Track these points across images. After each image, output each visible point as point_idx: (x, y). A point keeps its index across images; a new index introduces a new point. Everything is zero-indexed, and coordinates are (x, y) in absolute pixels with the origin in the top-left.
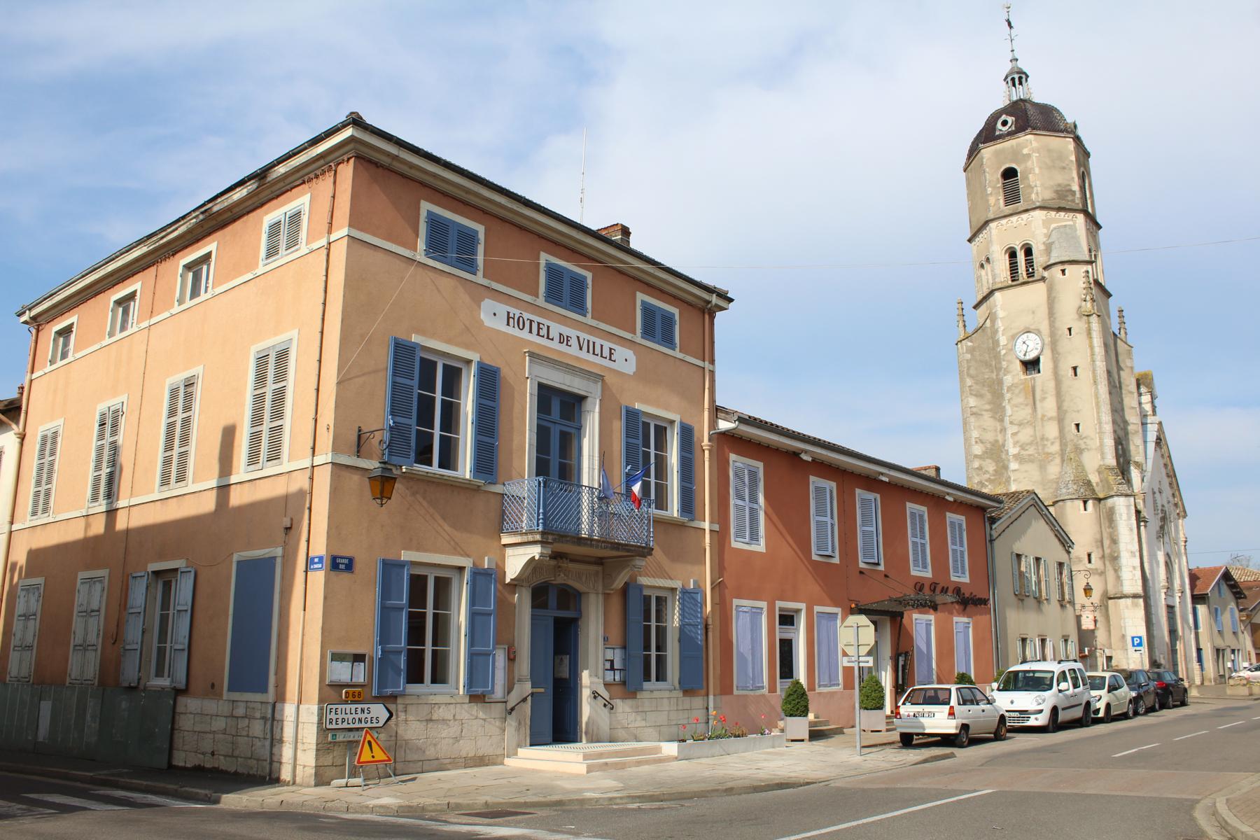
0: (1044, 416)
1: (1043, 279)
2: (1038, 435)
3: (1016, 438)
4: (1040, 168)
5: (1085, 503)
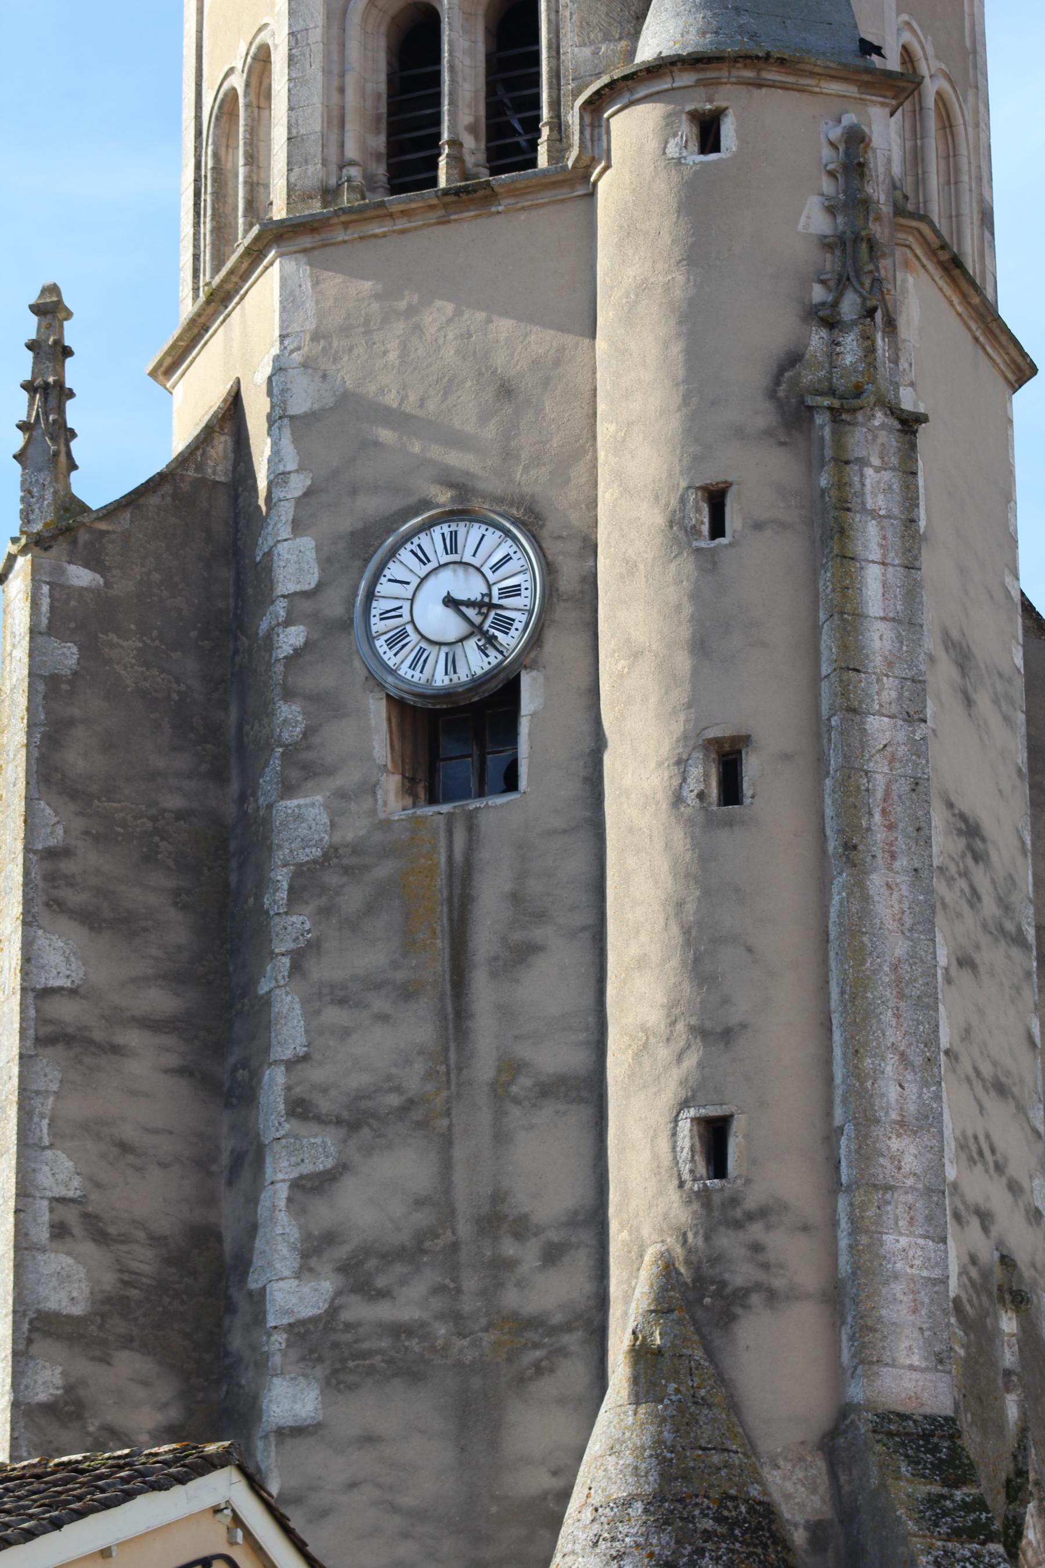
0: (511, 1068)
3: (323, 1214)
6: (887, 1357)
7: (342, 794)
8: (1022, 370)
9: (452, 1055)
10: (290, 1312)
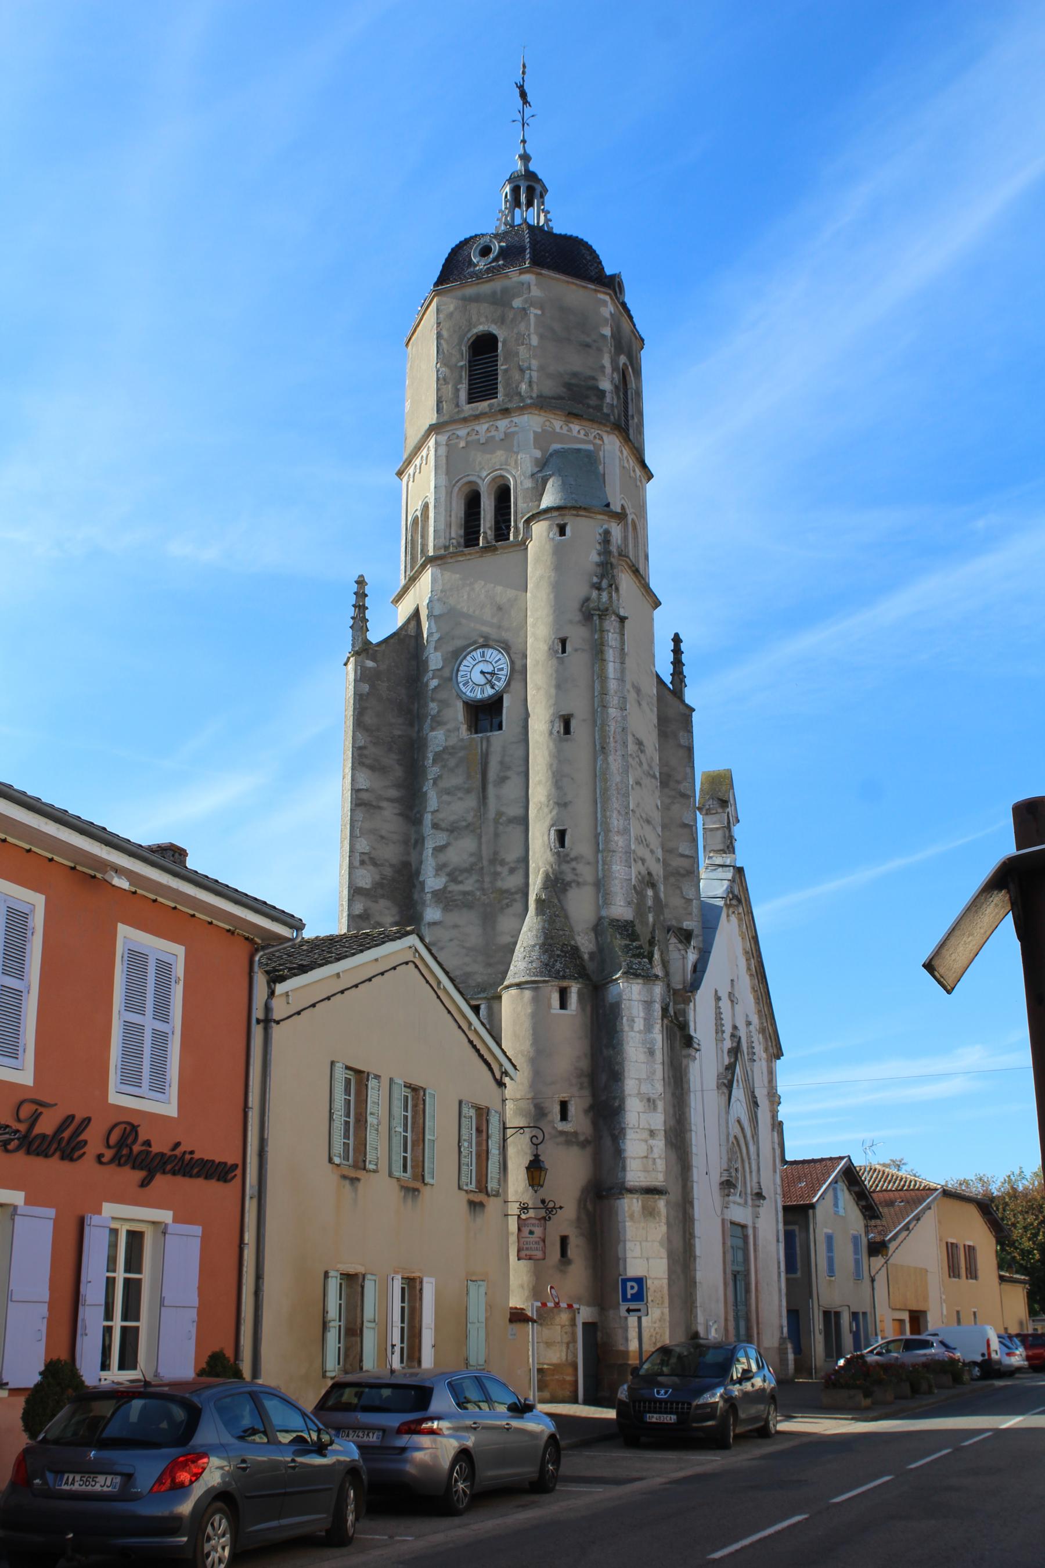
0: (500, 814)
3: (442, 858)
4: (541, 337)
7: (449, 731)
8: (657, 604)
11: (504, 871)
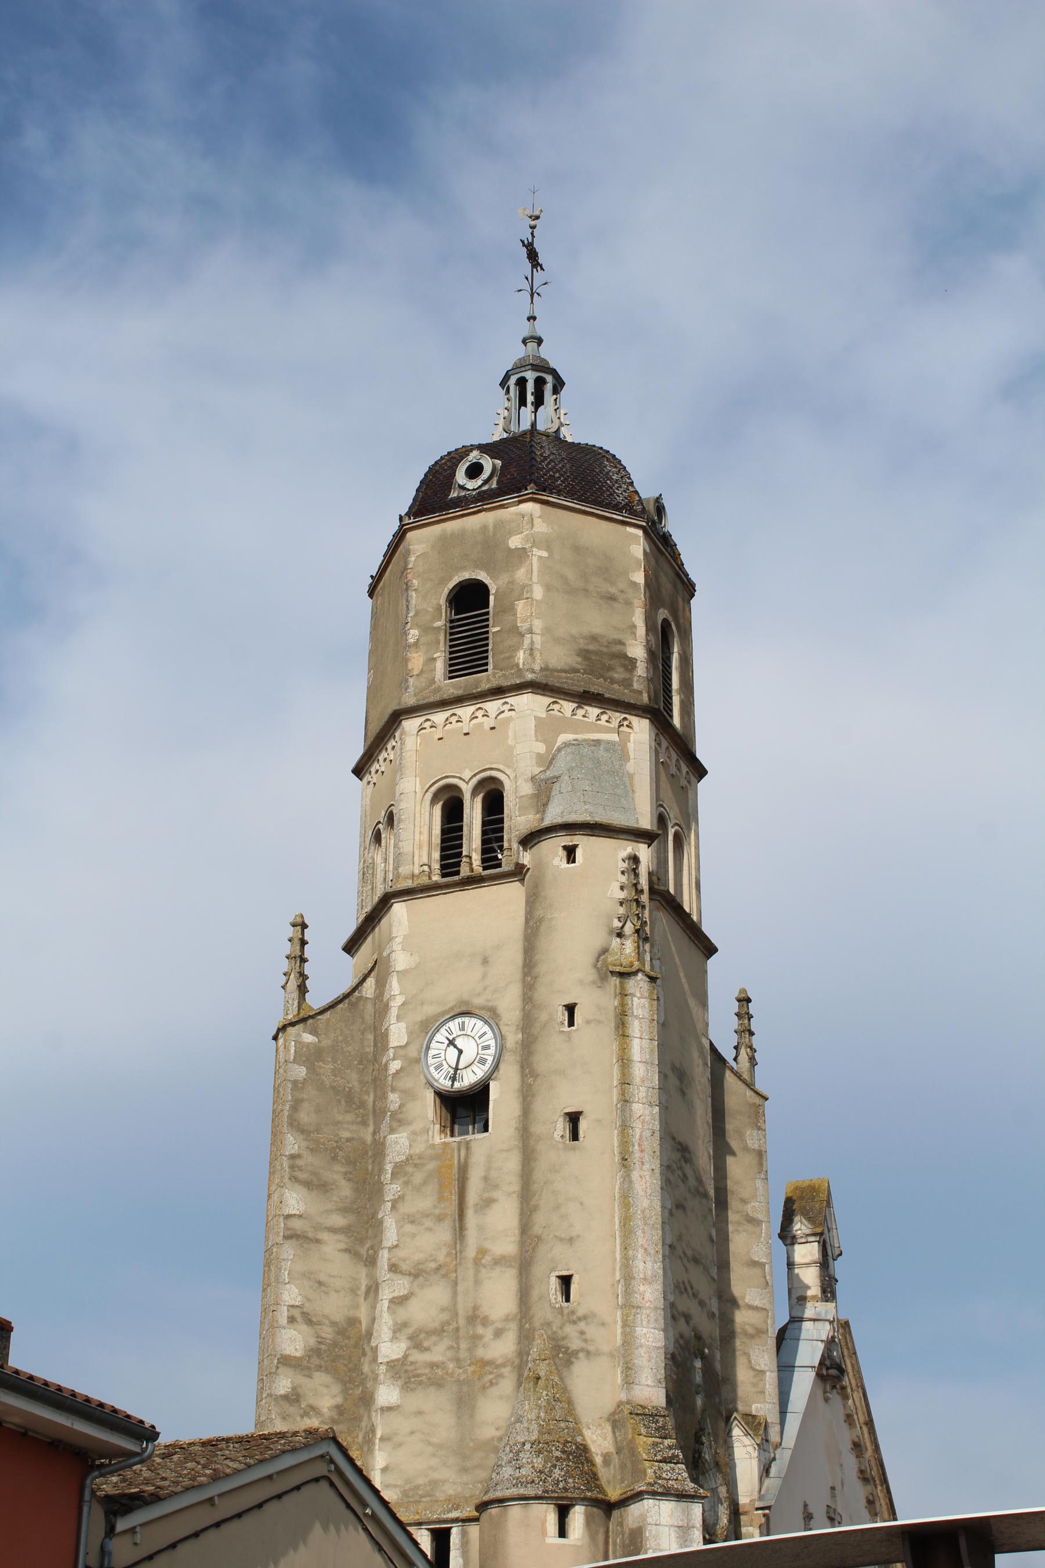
0: (482, 1252)
1: (519, 872)
2: (463, 1307)
3: (402, 1314)
4: (548, 588)
5: (563, 1513)
6: (636, 1381)
7: (414, 1133)
8: (710, 950)
9: (458, 1246)
10: (388, 1356)
11: (488, 1333)
